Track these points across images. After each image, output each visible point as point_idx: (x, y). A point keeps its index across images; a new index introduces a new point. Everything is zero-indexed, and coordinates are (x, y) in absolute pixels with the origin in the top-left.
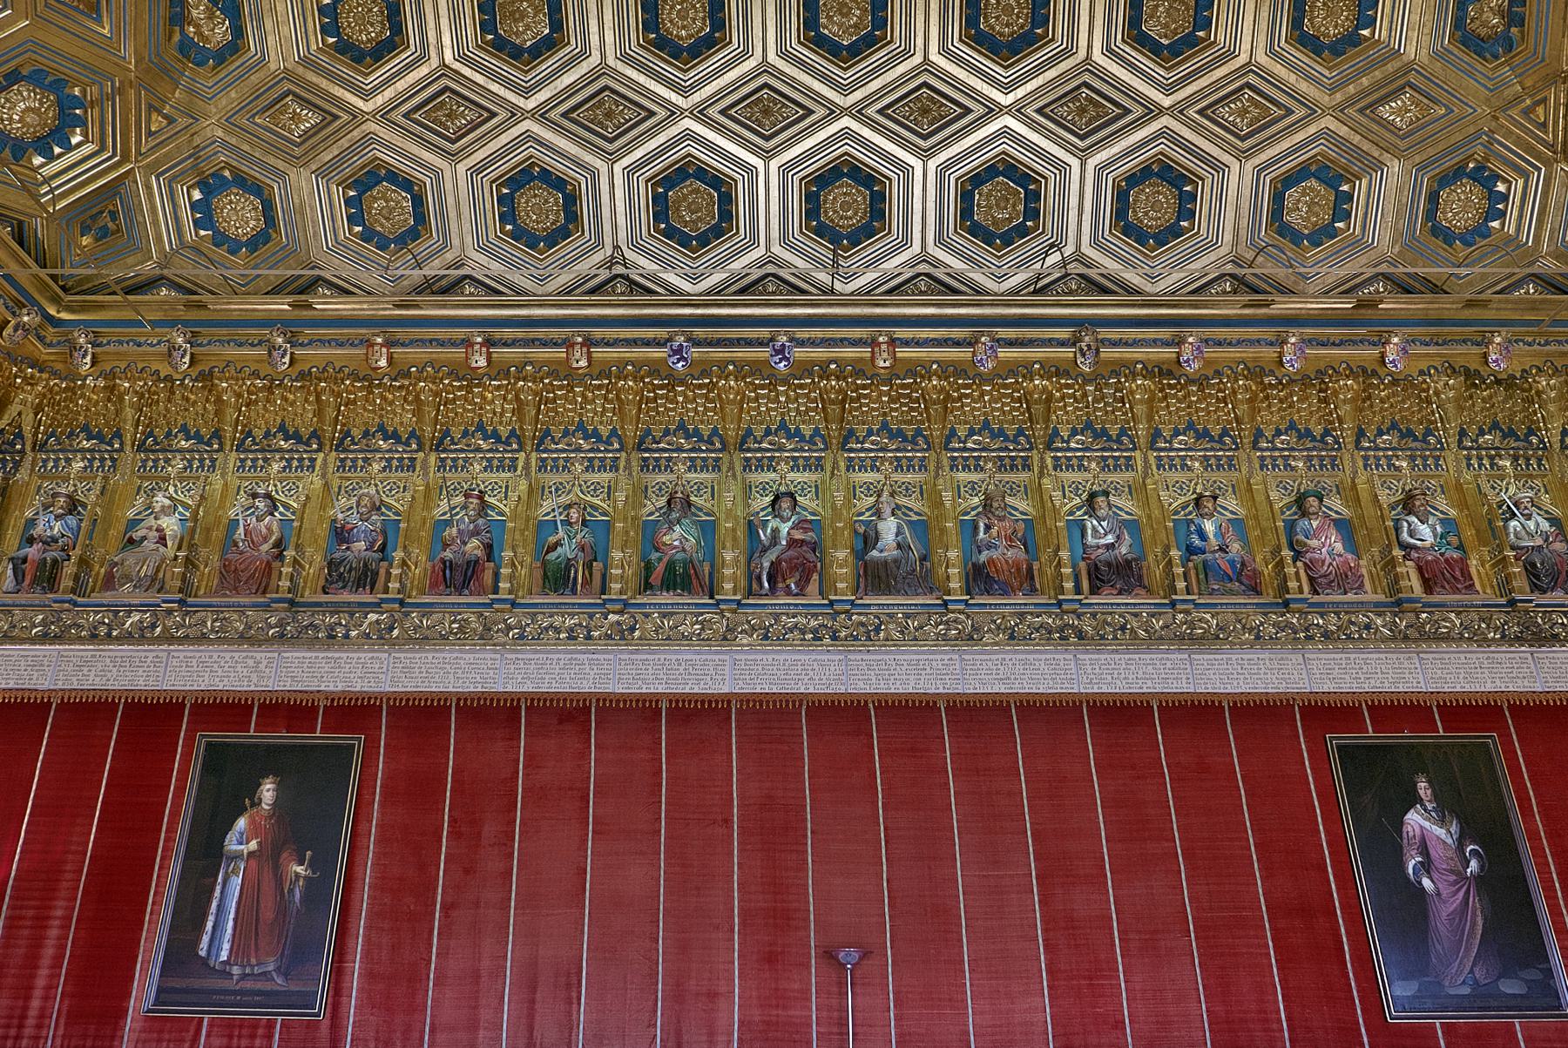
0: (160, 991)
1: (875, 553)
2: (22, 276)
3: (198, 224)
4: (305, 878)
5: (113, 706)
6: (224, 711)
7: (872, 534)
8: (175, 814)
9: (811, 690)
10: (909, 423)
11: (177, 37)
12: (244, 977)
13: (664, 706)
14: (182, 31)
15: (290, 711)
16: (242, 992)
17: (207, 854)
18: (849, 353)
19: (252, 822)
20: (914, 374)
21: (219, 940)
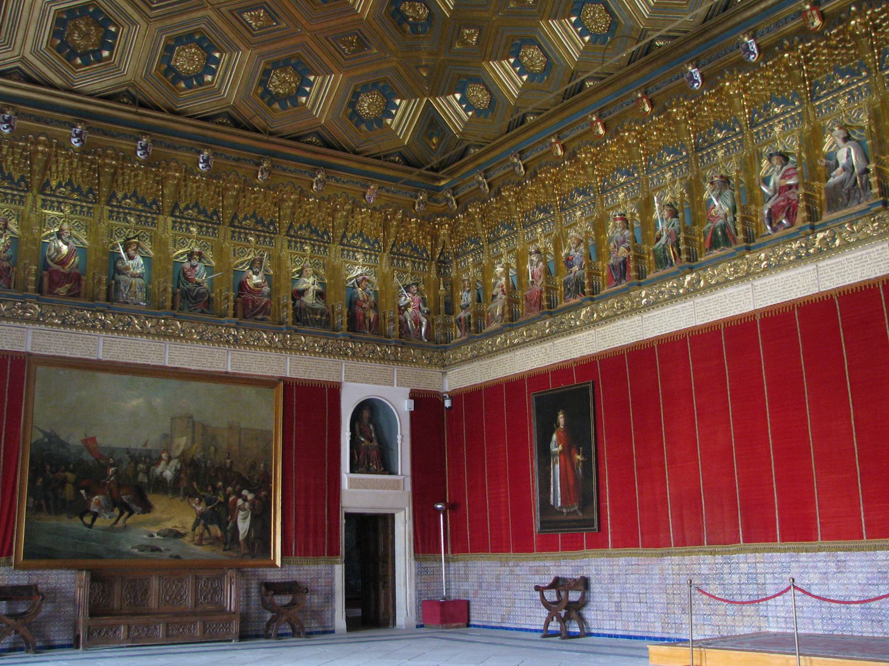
0: (541, 523)
1: (831, 180)
2: (413, 178)
3: (466, 110)
4: (582, 461)
5: (570, 369)
6: (537, 378)
7: (832, 162)
8: (531, 436)
9: (799, 296)
10: (851, 60)
11: (408, 29)
12: (568, 513)
13: (758, 318)
14: (409, 23)
15: (561, 372)
16: (569, 521)
17: (545, 455)
18: (791, 26)
19: (558, 436)
20: (841, 21)
21: (556, 497)
